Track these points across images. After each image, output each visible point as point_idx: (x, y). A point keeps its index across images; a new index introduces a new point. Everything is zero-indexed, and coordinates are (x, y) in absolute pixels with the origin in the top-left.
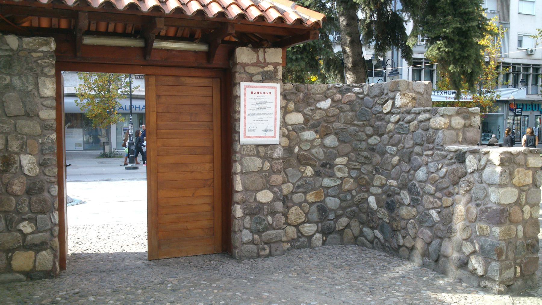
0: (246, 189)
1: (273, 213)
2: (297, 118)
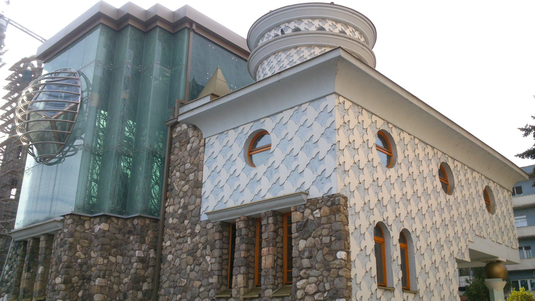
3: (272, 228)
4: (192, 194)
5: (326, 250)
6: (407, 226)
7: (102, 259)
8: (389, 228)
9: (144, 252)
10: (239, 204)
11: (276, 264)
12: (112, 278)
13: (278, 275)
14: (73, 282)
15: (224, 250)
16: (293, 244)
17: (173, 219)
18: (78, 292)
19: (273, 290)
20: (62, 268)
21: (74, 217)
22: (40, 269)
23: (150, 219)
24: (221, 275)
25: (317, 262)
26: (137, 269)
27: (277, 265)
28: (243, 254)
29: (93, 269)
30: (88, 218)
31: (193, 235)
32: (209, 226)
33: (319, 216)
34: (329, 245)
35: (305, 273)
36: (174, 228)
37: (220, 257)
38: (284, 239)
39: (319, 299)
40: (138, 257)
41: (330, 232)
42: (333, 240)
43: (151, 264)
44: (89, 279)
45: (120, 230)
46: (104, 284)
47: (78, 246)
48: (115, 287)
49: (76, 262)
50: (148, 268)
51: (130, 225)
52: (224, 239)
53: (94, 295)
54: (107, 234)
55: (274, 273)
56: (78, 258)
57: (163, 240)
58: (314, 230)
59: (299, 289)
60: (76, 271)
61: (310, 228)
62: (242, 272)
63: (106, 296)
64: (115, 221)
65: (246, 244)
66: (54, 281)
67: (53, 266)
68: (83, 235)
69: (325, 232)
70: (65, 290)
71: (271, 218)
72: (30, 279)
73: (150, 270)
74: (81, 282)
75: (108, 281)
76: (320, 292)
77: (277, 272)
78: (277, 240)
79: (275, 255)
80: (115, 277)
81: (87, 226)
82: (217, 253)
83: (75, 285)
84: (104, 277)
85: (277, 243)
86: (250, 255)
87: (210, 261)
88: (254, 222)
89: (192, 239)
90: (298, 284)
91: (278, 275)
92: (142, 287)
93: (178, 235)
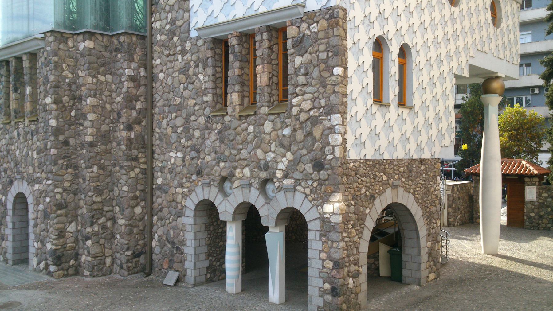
0: (527, 212)
1: (535, 219)
2: (545, 195)
3: (266, 44)
4: (179, 8)
5: (323, 66)
6: (407, 41)
7: (91, 78)
8: (388, 42)
9: (133, 70)
10: (230, 18)
11: (271, 82)
12: (104, 97)
13: (273, 92)
14: (64, 102)
15: (217, 68)
16: (289, 61)
17: (161, 36)
18: (71, 112)
19: (269, 107)
20: (50, 88)
21: (55, 35)
22: (28, 90)
23: (137, 35)
24: (216, 94)
25: (313, 79)
26: (129, 88)
27: (273, 82)
28: (237, 72)
29: (83, 88)
30: (71, 36)
31: (184, 52)
32: (200, 43)
33: (316, 30)
34: (325, 61)
35: (301, 90)
36: (163, 45)
37: (213, 75)
38: (279, 56)
39: (315, 115)
40: (128, 76)
41: (327, 48)
42: (330, 56)
43: (142, 82)
44: (80, 99)
45: (106, 48)
46: (96, 104)
47: (64, 66)
48: (108, 106)
49: (64, 82)
50: (140, 87)
51: (116, 42)
52: (216, 57)
53: (87, 114)
54: (93, 51)
55: (269, 90)
56: (66, 77)
57: (153, 58)
58: (311, 45)
59: (294, 106)
60: (65, 91)
61: (307, 43)
62: (236, 90)
63: (99, 116)
64: (100, 38)
65: (240, 61)
66: (44, 102)
67: (40, 86)
68: (67, 53)
69: (322, 47)
70: (56, 110)
71: (265, 34)
72: (19, 100)
73: (142, 89)
74: (72, 101)
75: (100, 100)
76: (316, 108)
77: (272, 90)
78: (272, 57)
79: (270, 73)
80: (106, 97)
81: (70, 43)
82: (210, 71)
83: (67, 105)
84: (95, 96)
85: (272, 60)
86: (244, 73)
87: (204, 79)
88: (247, 38)
89: (183, 57)
90: (294, 101)
91: (273, 92)
92: (135, 105)
93: (167, 52)
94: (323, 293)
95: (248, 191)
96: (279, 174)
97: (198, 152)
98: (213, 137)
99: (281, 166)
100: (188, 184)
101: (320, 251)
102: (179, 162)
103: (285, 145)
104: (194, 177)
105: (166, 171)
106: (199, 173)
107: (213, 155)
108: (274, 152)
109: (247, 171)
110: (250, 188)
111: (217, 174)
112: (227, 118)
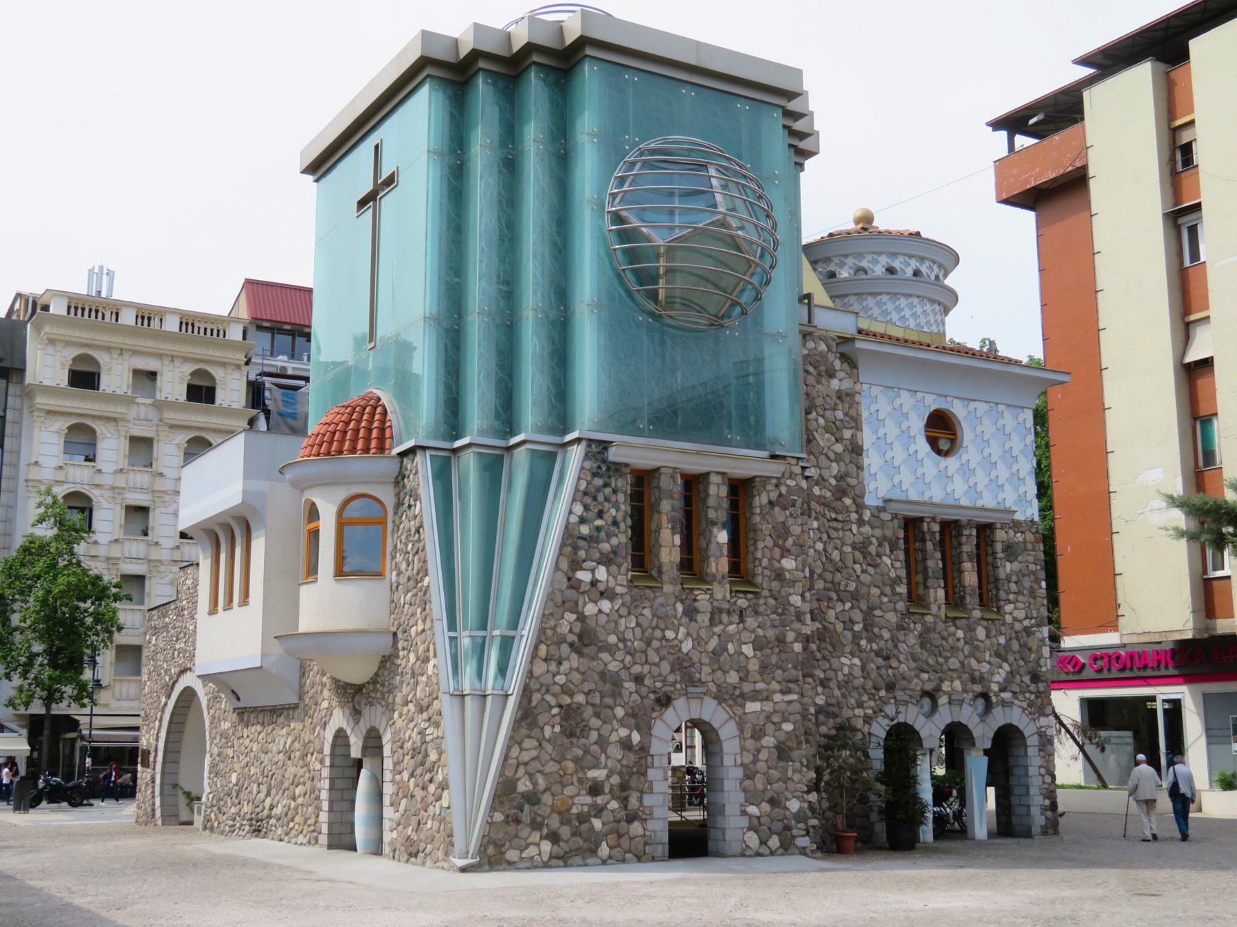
5: (1032, 578)
10: (926, 498)
31: (861, 522)
88: (951, 529)
93: (834, 516)
94: (1044, 809)
95: (958, 708)
96: (995, 687)
97: (887, 658)
98: (912, 640)
99: (998, 678)
100: (872, 703)
101: (1040, 767)
102: (857, 672)
103: (1001, 655)
104: (883, 693)
105: (833, 684)
106: (890, 687)
107: (912, 664)
108: (989, 663)
109: (957, 684)
110: (961, 705)
111: (919, 688)
112: (929, 619)
